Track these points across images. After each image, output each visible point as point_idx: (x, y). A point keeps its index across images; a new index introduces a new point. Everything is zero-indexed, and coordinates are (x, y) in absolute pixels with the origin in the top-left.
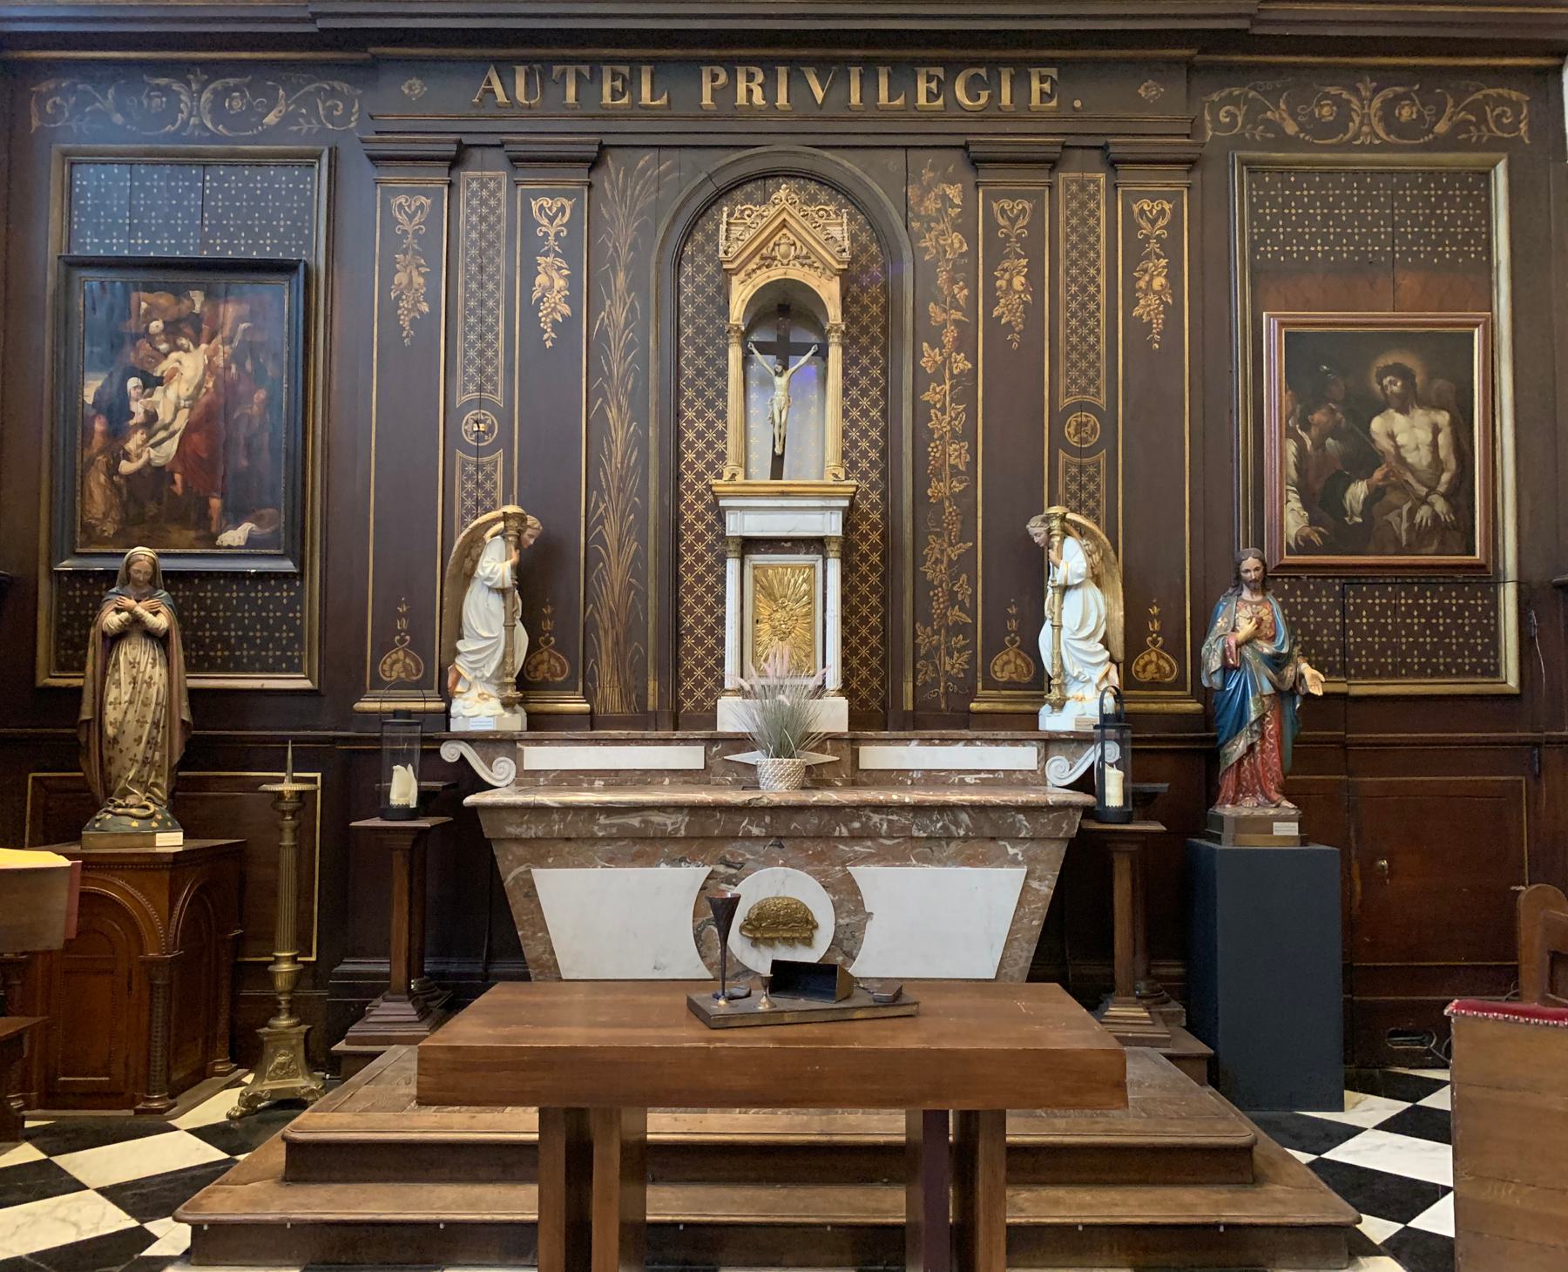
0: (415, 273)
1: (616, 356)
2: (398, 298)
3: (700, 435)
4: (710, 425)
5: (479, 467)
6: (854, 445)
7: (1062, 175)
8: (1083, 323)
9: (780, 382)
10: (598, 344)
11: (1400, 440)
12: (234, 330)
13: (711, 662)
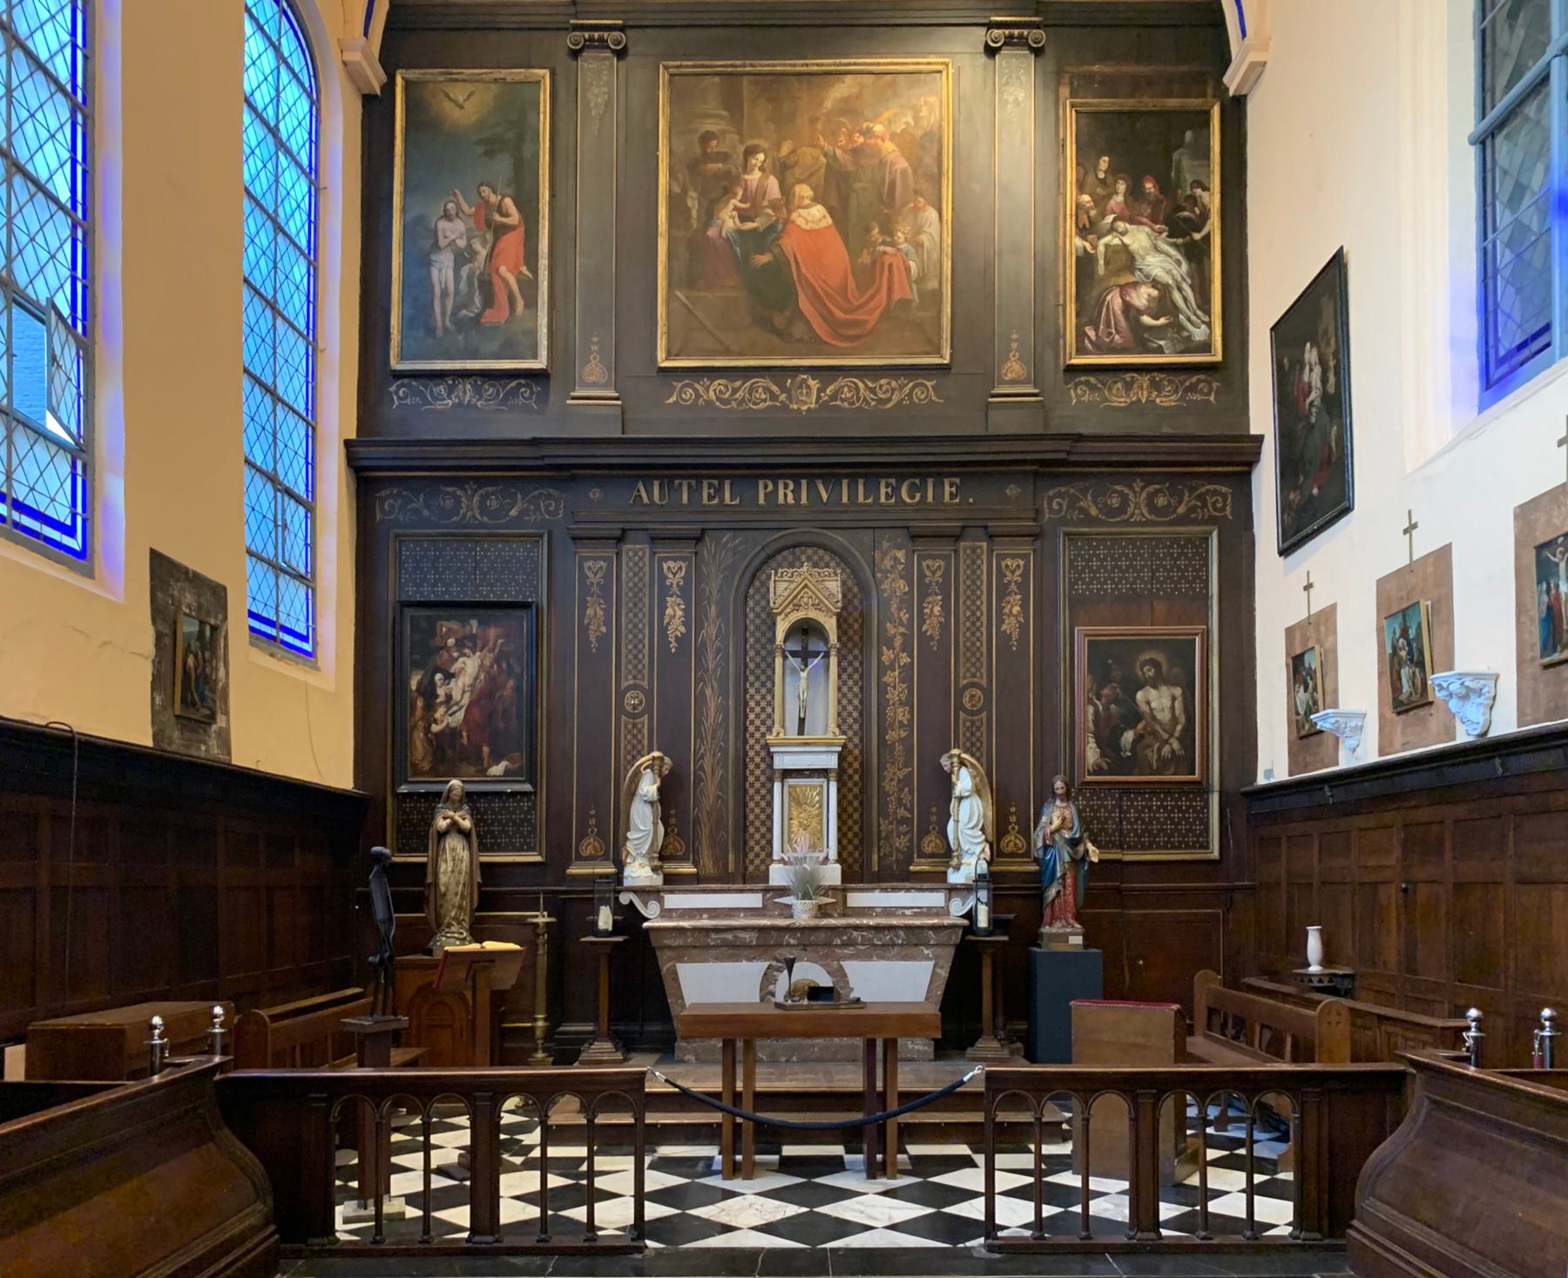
1: (710, 656)
3: (758, 704)
4: (763, 697)
5: (634, 725)
6: (844, 708)
8: (973, 634)
9: (804, 675)
10: (701, 650)
11: (1154, 705)
13: (763, 842)
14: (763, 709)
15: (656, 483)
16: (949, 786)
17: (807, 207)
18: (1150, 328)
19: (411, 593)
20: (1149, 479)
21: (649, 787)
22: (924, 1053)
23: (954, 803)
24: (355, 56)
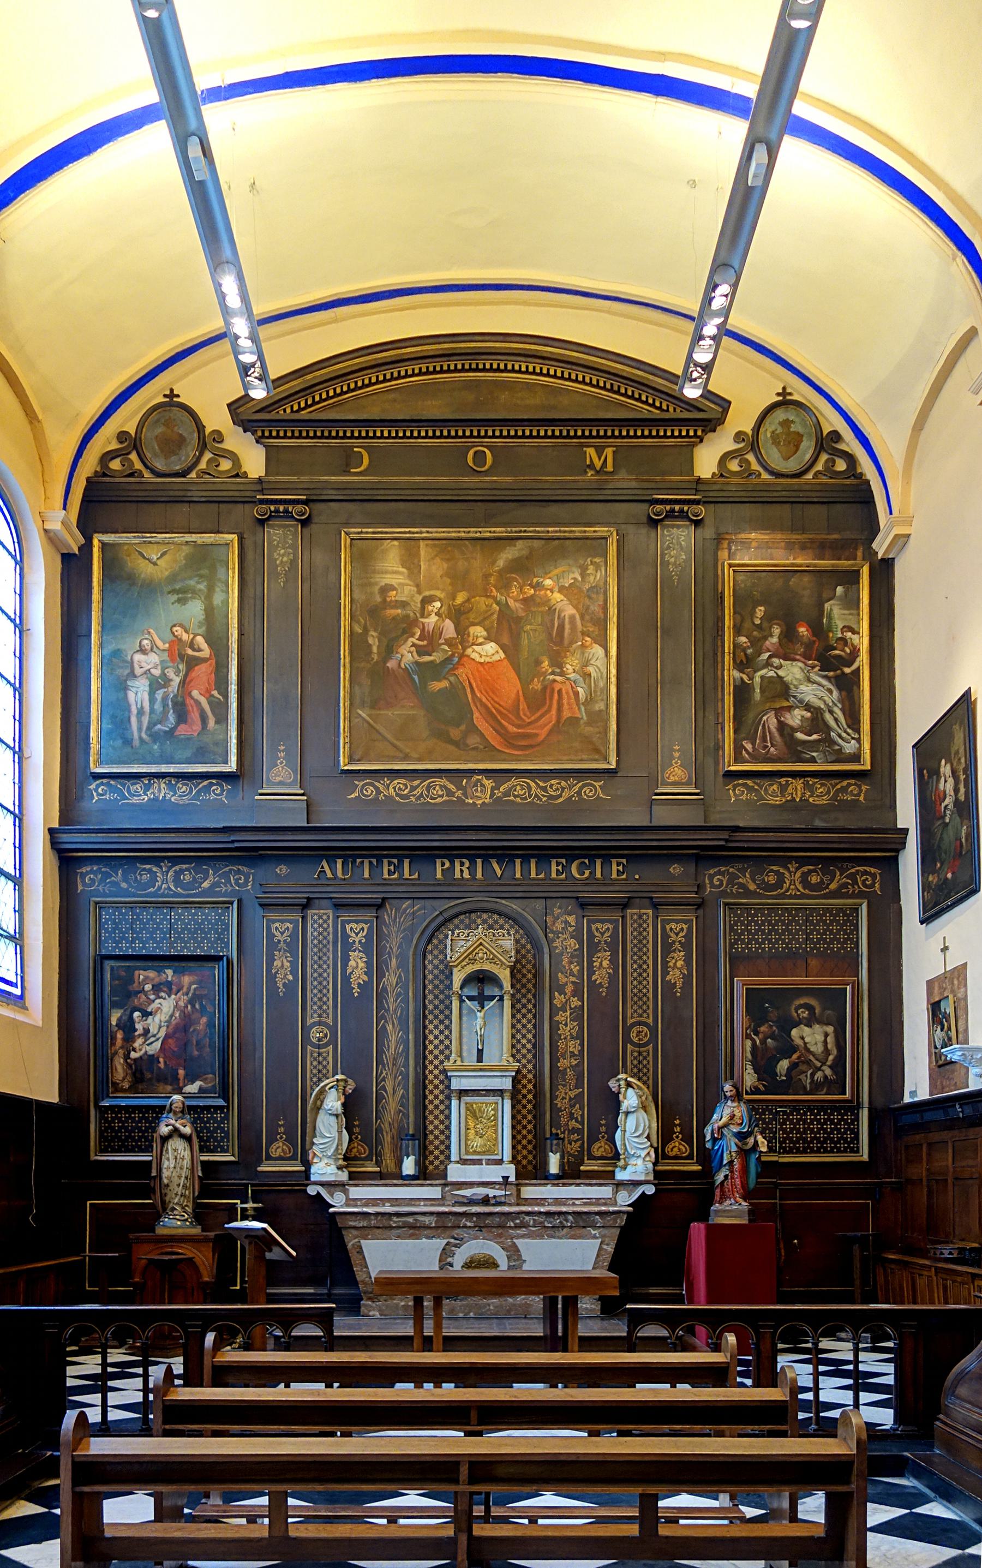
0: (285, 961)
1: (391, 1000)
2: (277, 973)
3: (436, 1037)
5: (319, 1054)
7: (629, 911)
10: (381, 995)
12: (189, 989)
14: (441, 1042)
15: (339, 862)
16: (618, 1104)
17: (480, 644)
18: (805, 742)
19: (109, 948)
20: (802, 862)
21: (333, 1102)
22: (592, 1310)
23: (621, 1117)
24: (55, 526)
